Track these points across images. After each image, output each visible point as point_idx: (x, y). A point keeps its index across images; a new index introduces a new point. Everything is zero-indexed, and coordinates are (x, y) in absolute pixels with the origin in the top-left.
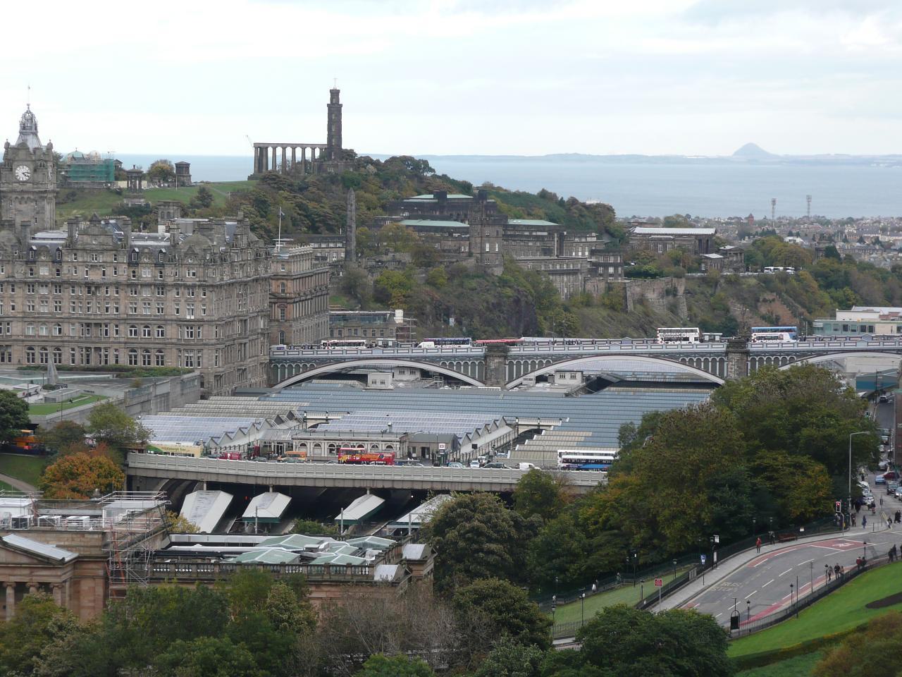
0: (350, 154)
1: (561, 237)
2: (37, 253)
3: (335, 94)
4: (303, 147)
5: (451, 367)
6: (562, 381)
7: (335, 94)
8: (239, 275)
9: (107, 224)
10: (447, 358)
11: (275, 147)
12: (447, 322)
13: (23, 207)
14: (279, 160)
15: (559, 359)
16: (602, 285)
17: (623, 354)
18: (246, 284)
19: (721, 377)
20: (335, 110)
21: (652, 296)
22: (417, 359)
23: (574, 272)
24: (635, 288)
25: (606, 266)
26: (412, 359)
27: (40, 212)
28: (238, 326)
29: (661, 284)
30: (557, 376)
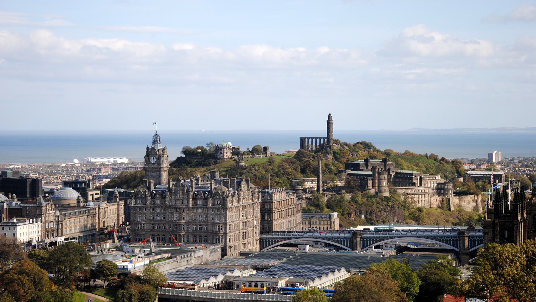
0: (337, 142)
1: (421, 178)
2: (155, 194)
3: (329, 116)
4: (320, 138)
5: (337, 242)
6: (386, 248)
7: (329, 116)
8: (243, 202)
9: (185, 181)
10: (336, 238)
11: (308, 138)
12: (360, 217)
13: (154, 174)
14: (318, 144)
15: (384, 239)
16: (439, 198)
17: (413, 237)
18: (245, 207)
19: (457, 247)
20: (329, 123)
21: (463, 204)
22: (323, 238)
23: (425, 194)
24: (454, 200)
25: (445, 190)
26: (320, 238)
27: (160, 176)
28: (241, 224)
29: (470, 198)
30: (384, 246)
